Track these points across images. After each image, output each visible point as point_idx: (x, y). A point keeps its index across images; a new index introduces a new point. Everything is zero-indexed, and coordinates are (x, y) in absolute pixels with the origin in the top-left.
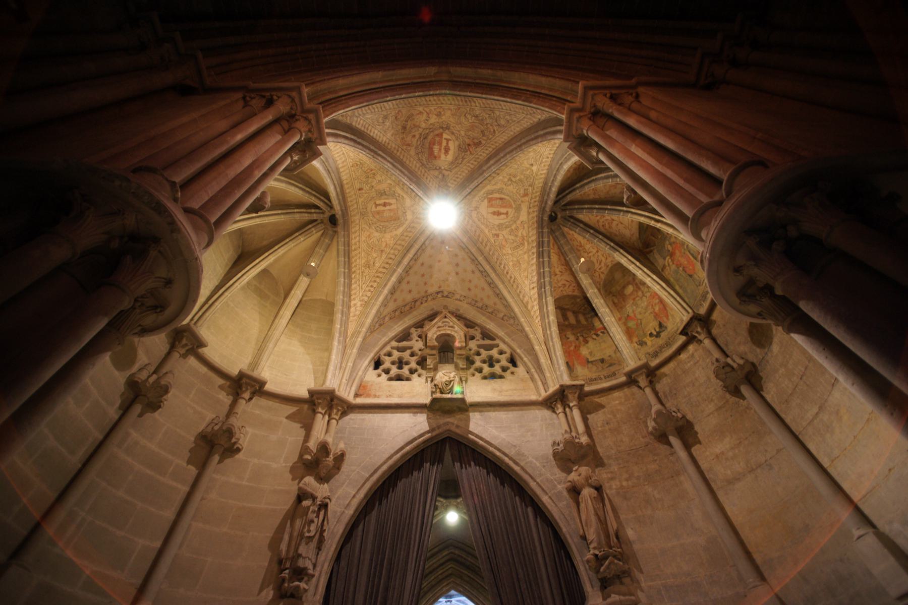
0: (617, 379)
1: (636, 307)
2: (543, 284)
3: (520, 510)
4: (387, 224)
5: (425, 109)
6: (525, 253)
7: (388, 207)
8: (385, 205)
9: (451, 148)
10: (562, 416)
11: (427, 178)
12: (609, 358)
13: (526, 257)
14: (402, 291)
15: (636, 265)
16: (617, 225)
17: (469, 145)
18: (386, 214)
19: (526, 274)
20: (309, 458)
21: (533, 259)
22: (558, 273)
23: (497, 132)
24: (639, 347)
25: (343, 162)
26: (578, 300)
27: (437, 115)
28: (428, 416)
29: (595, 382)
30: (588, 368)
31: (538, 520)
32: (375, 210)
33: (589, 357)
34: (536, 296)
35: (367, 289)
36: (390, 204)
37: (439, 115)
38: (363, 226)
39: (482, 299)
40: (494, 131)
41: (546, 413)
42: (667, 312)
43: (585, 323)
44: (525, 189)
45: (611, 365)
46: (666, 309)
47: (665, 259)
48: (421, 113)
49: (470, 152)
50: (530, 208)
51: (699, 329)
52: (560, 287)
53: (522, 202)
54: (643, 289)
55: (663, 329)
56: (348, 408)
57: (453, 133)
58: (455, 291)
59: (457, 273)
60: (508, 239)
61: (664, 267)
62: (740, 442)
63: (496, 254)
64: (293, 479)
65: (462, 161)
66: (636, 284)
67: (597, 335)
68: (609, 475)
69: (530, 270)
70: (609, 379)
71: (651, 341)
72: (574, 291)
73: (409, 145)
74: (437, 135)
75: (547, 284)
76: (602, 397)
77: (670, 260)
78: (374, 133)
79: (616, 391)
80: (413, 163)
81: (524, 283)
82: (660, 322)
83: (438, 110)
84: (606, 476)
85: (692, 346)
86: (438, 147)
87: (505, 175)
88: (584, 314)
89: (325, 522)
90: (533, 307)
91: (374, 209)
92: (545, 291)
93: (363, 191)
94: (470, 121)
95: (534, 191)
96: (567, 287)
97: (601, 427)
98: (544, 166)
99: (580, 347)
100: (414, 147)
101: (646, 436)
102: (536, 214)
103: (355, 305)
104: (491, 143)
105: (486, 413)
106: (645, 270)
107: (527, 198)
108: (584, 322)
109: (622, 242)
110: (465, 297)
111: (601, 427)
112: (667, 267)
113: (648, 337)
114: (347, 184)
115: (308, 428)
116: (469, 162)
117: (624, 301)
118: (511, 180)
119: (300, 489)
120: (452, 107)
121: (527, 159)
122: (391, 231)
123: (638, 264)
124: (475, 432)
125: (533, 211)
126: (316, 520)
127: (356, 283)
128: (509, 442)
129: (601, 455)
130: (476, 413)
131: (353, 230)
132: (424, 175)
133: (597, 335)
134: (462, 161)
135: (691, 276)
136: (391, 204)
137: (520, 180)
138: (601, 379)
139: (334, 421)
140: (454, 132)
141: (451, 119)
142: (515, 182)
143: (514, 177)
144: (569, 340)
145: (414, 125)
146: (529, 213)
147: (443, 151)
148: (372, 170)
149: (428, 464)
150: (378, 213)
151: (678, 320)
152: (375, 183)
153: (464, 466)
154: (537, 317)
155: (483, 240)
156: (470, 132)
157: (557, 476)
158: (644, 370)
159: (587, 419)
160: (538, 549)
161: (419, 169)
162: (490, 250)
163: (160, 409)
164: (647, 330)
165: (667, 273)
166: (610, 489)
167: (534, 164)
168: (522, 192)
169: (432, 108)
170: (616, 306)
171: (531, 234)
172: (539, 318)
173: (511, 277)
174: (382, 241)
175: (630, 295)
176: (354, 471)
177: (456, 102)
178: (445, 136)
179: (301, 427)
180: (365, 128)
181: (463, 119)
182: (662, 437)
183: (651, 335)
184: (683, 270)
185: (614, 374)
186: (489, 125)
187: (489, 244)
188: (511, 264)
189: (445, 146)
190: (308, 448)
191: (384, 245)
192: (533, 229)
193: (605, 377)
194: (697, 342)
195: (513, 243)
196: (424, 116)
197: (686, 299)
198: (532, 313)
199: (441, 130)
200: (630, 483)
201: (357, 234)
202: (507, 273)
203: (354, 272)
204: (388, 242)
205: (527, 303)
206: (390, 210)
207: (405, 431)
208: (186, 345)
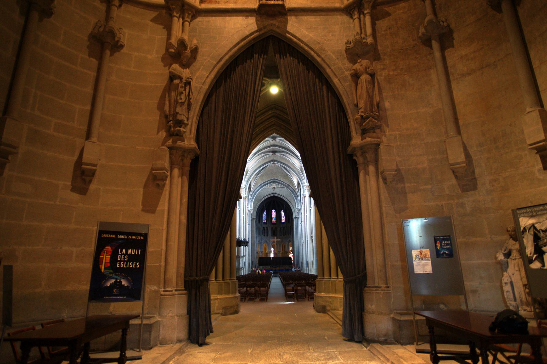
3: (318, 87)
10: (357, 21)
20: (173, 51)
28: (256, 18)
31: (329, 94)
41: (345, 18)
56: (197, 13)
62: (482, 48)
64: (165, 66)
68: (382, 67)
76: (391, 6)
84: (379, 67)
89: (191, 94)
97: (384, 31)
101: (415, 40)
105: (300, 17)
111: (384, 31)
115: (169, 28)
119: (170, 72)
124: (291, 32)
126: (184, 92)
128: (315, 40)
129: (380, 52)
130: (292, 17)
139: (187, 23)
149: (257, 55)
153: (282, 57)
157: (347, 65)
159: (376, 24)
160: (327, 111)
163: (53, 16)
166: (381, 76)
176: (206, 60)
179: (163, 28)
182: (427, 42)
190: (171, 44)
200: (395, 73)
207: (240, 30)
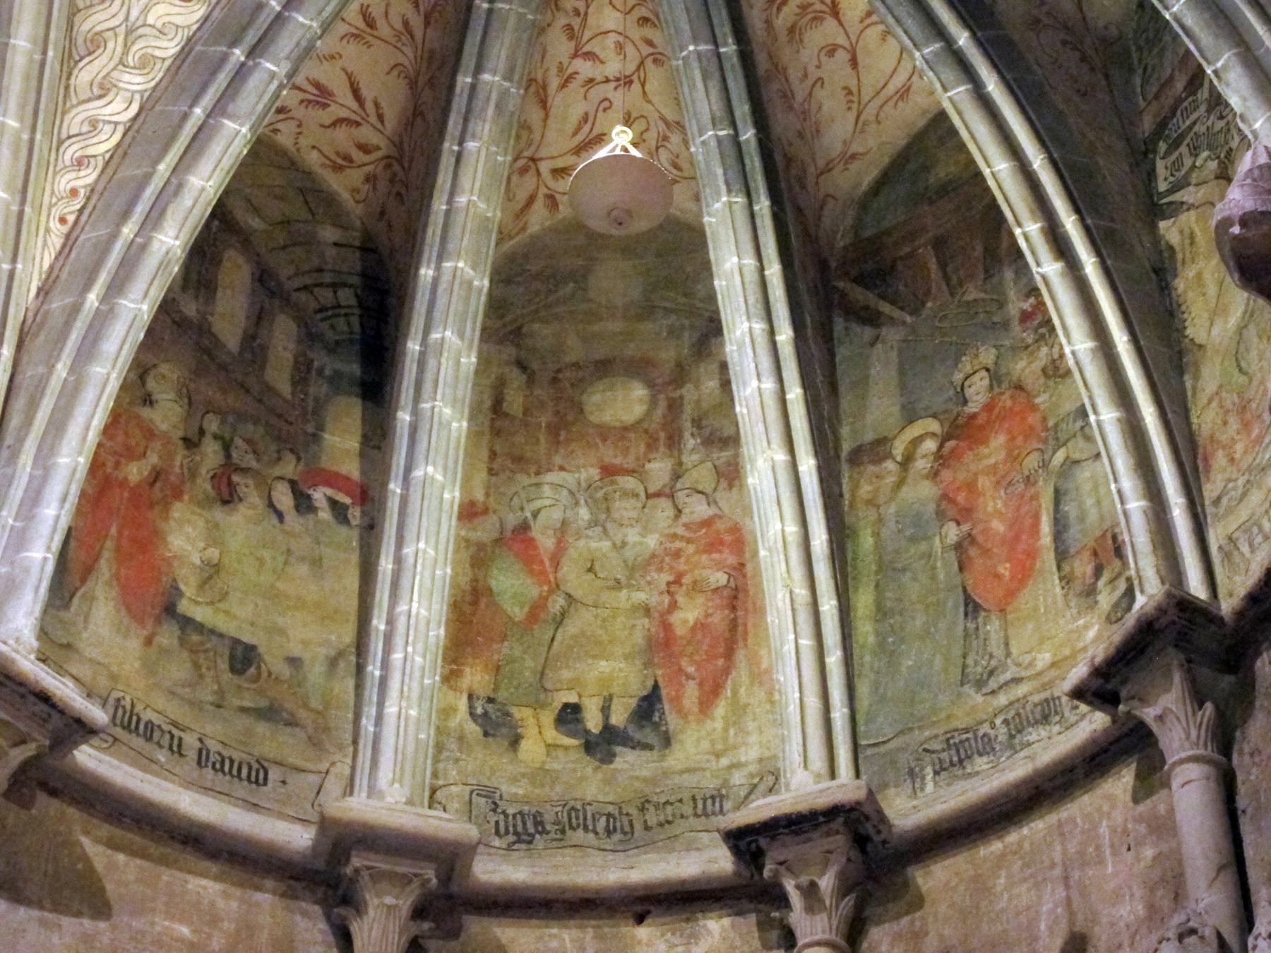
0: (255, 807)
1: (594, 523)
2: (263, 21)
12: (285, 671)
15: (772, 332)
16: (832, 50)
24: (473, 729)
26: (329, 234)
29: (138, 742)
30: (149, 642)
33: (188, 590)
34: (169, 48)
42: (727, 671)
43: (285, 388)
45: (270, 714)
46: (729, 653)
47: (910, 417)
51: (826, 883)
54: (689, 459)
55: (648, 736)
61: (876, 450)
66: (675, 407)
67: (303, 503)
70: (222, 781)
71: (551, 747)
72: (342, 163)
75: (286, 43)
77: (930, 445)
79: (214, 868)
82: (656, 687)
85: (726, 921)
88: (309, 337)
90: (104, 89)
92: (241, 73)
96: (326, 116)
99: (177, 494)
106: (795, 393)
108: (279, 376)
109: (789, 160)
112: (889, 465)
113: (548, 718)
117: (554, 431)
123: (785, 335)
133: (303, 503)
135: (972, 607)
138: (177, 749)
144: (146, 412)
151: (750, 754)
154: (80, 163)
158: (430, 873)
164: (566, 674)
165: (865, 490)
170: (496, 432)
172: (88, 177)
175: (605, 433)
183: (569, 716)
184: (958, 547)
185: (257, 774)
193: (202, 758)
194: (763, 926)
197: (863, 689)
198: (75, 120)
205: (96, 43)
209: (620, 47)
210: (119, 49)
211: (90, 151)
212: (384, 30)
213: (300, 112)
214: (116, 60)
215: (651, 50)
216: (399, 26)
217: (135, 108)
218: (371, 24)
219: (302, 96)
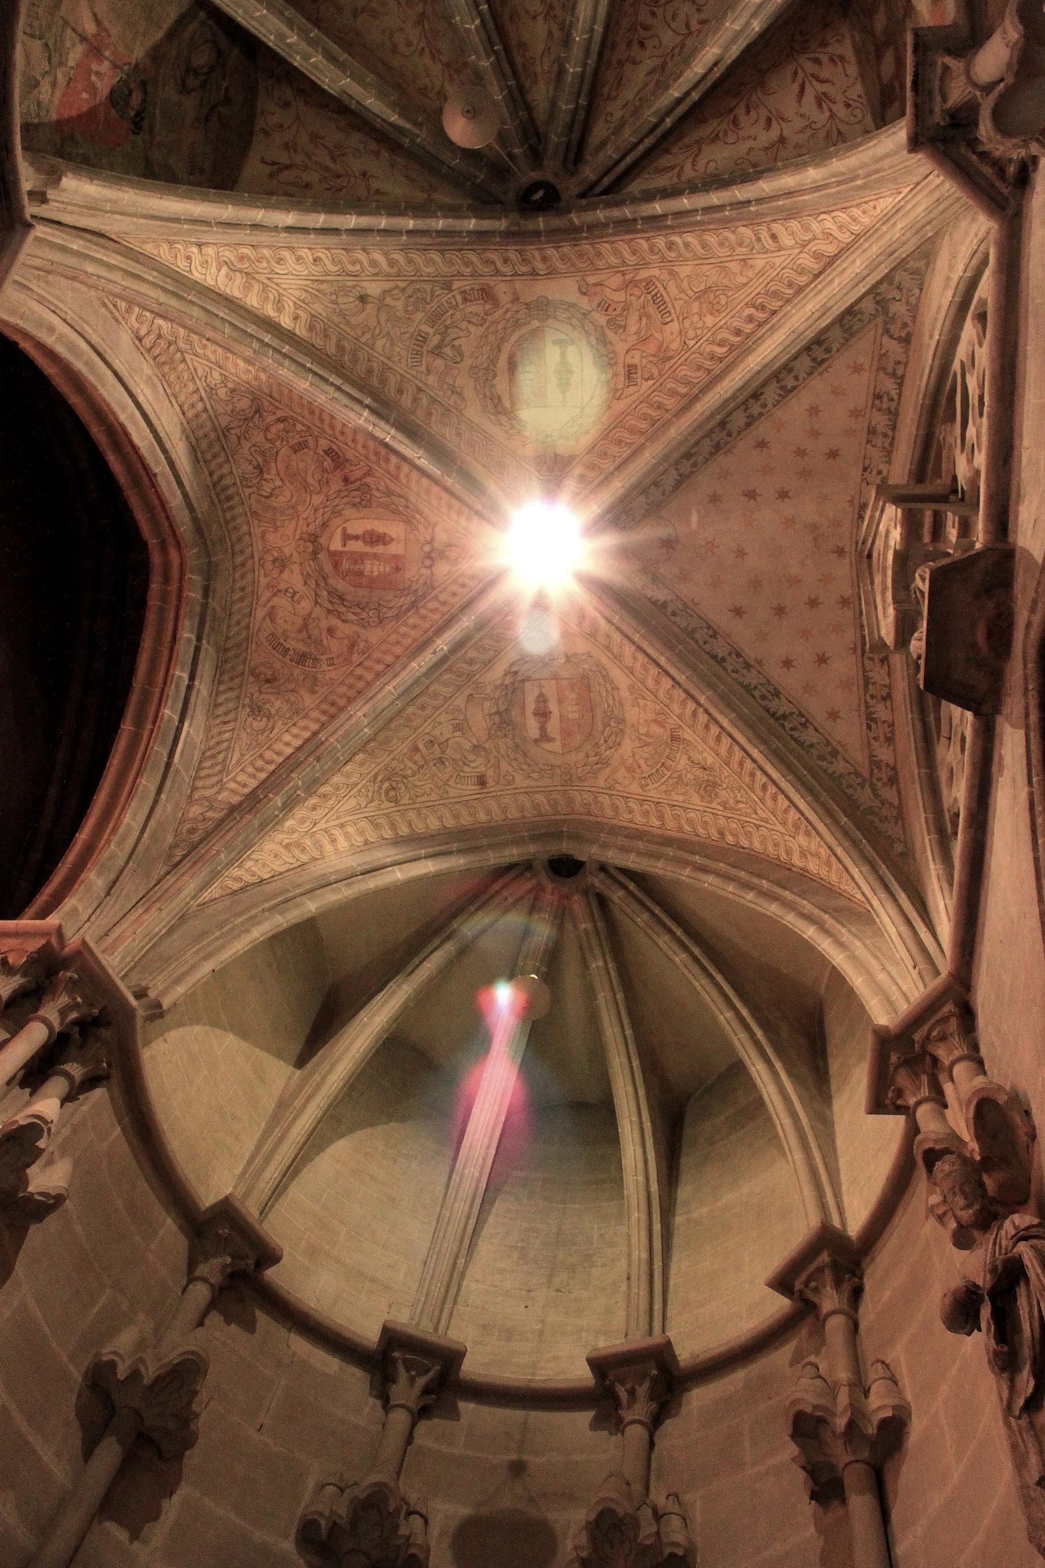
4: (599, 713)
5: (263, 600)
6: (672, 274)
7: (553, 707)
8: (543, 714)
9: (369, 528)
11: (454, 594)
13: (684, 270)
14: (808, 688)
17: (346, 480)
18: (573, 712)
19: (735, 267)
21: (687, 245)
22: (774, 134)
23: (280, 414)
25: (377, 826)
27: (283, 568)
32: (558, 743)
35: (769, 803)
36: (542, 699)
37: (281, 563)
38: (601, 783)
39: (855, 414)
40: (279, 420)
44: (465, 300)
48: (271, 615)
49: (365, 475)
50: (534, 273)
52: (833, 116)
53: (516, 299)
57: (325, 525)
58: (851, 502)
59: (784, 495)
60: (638, 333)
63: (683, 371)
65: (399, 496)
69: (722, 252)
73: (353, 645)
74: (336, 566)
78: (287, 744)
80: (404, 635)
81: (761, 273)
83: (269, 565)
86: (367, 562)
87: (423, 368)
90: (828, 235)
91: (556, 746)
93: (490, 773)
94: (278, 483)
95: (467, 271)
98: (354, 263)
100: (362, 631)
102: (551, 252)
103: (803, 854)
104: (318, 423)
107: (501, 289)
110: (865, 469)
114: (456, 817)
116: (397, 477)
118: (439, 346)
120: (257, 531)
121: (344, 316)
122: (621, 703)
125: (544, 259)
127: (749, 835)
131: (610, 813)
132: (444, 603)
134: (399, 496)
136: (541, 695)
137: (434, 319)
140: (320, 519)
141: (289, 531)
142: (443, 335)
143: (425, 340)
145: (300, 631)
146: (553, 273)
147: (379, 549)
148: (416, 749)
150: (566, 734)
152: (461, 740)
155: (645, 417)
156: (310, 480)
161: (424, 618)
162: (674, 393)
167: (356, 293)
168: (476, 308)
169: (263, 581)
171: (613, 260)
172: (856, 212)
173: (750, 319)
174: (647, 735)
177: (239, 521)
178: (336, 545)
180: (261, 770)
181: (281, 501)
186: (270, 436)
187: (659, 398)
188: (709, 320)
189: (366, 543)
191: (655, 729)
192: (599, 255)
195: (649, 316)
196: (282, 603)
199: (322, 556)
201: (620, 803)
202: (738, 332)
203: (721, 834)
204: (651, 716)
205: (817, 256)
206: (560, 701)
208: (632, 1393)
209: (674, 18)
210: (812, 244)
211: (849, 220)
212: (763, 114)
213: (840, 98)
214: (817, 241)
215: (655, 9)
216: (753, 113)
217: (823, 216)
218: (769, 121)
219: (831, 105)
